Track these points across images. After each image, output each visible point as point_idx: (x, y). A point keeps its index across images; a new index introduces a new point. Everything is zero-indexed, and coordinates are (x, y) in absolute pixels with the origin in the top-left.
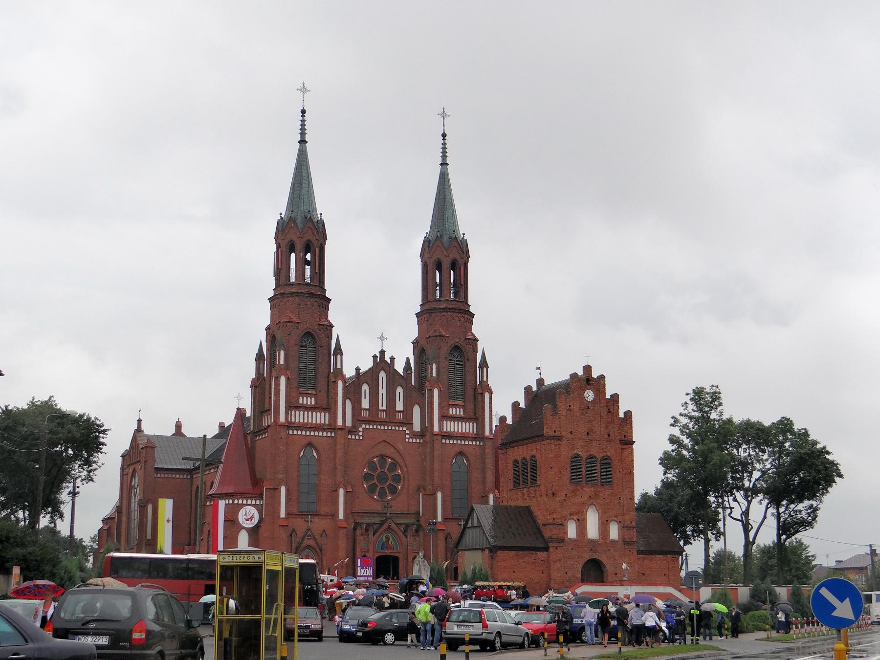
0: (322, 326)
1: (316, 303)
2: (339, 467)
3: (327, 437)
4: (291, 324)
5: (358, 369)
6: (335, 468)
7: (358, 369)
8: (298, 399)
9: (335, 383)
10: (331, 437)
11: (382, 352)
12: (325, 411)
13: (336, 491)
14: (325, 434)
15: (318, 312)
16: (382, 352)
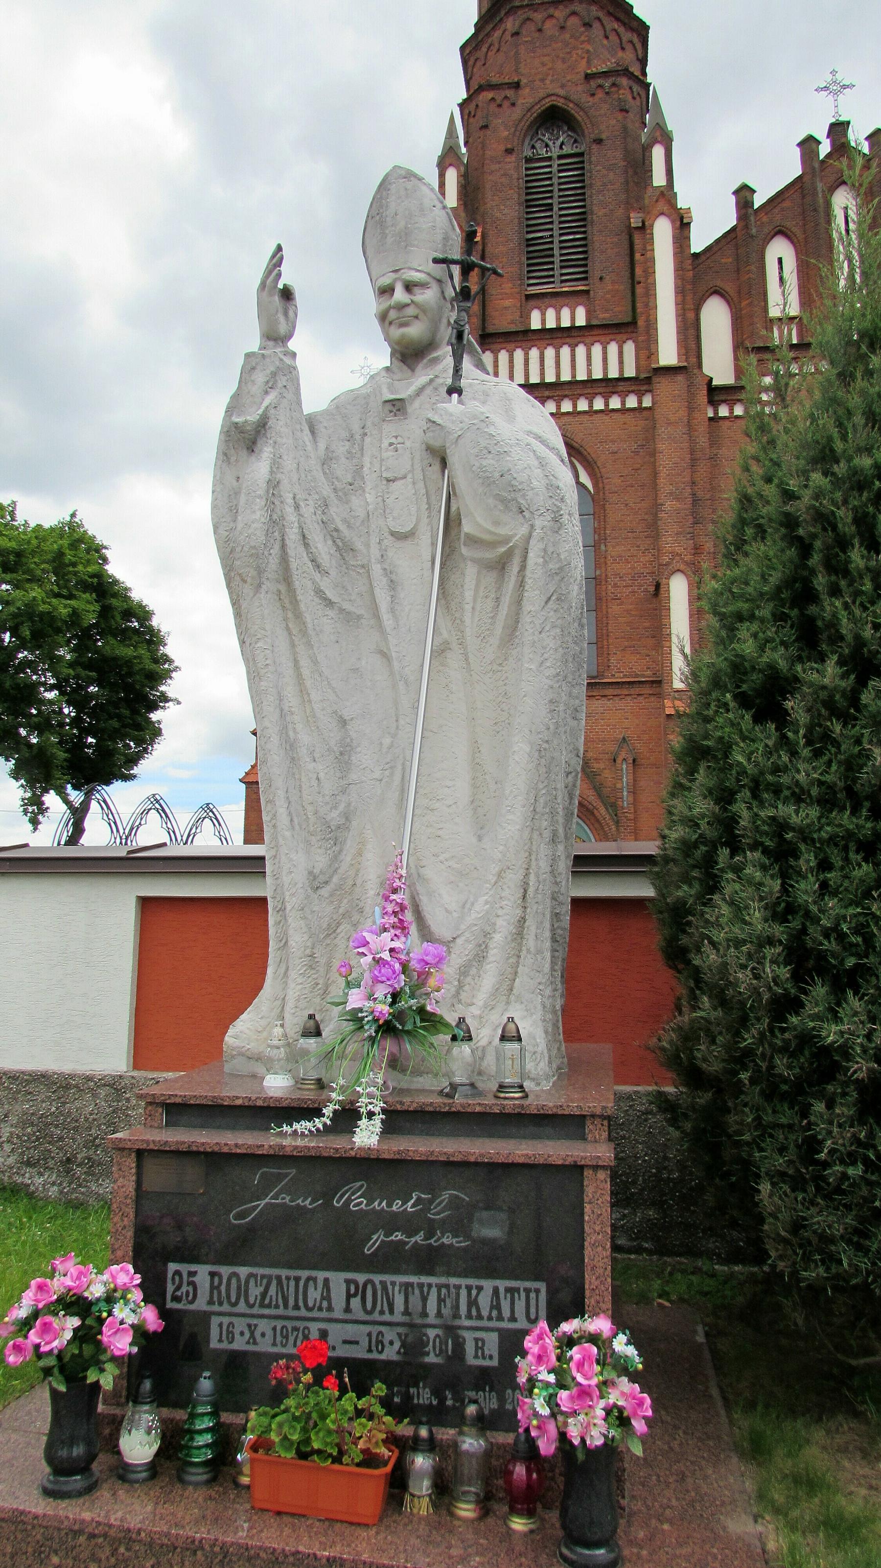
0: (600, 81)
1: (574, 21)
2: (669, 505)
3: (624, 410)
4: (490, 95)
5: (744, 193)
6: (656, 508)
7: (744, 193)
8: (528, 318)
9: (645, 229)
10: (640, 409)
11: (838, 129)
12: (619, 337)
13: (658, 591)
14: (615, 403)
15: (583, 42)
16: (838, 129)
